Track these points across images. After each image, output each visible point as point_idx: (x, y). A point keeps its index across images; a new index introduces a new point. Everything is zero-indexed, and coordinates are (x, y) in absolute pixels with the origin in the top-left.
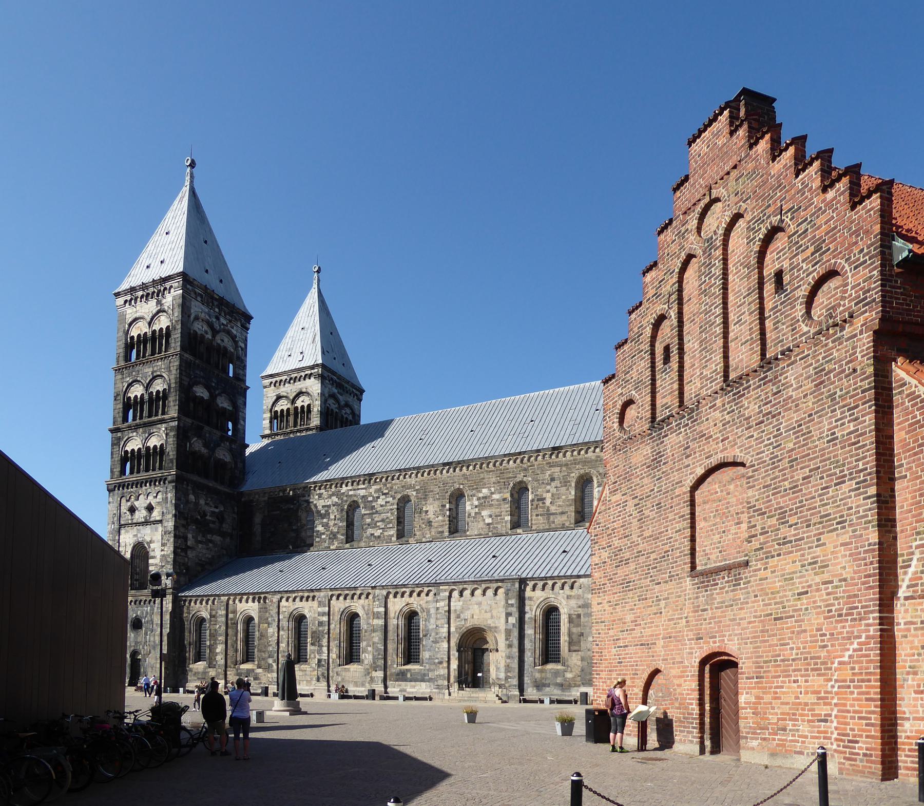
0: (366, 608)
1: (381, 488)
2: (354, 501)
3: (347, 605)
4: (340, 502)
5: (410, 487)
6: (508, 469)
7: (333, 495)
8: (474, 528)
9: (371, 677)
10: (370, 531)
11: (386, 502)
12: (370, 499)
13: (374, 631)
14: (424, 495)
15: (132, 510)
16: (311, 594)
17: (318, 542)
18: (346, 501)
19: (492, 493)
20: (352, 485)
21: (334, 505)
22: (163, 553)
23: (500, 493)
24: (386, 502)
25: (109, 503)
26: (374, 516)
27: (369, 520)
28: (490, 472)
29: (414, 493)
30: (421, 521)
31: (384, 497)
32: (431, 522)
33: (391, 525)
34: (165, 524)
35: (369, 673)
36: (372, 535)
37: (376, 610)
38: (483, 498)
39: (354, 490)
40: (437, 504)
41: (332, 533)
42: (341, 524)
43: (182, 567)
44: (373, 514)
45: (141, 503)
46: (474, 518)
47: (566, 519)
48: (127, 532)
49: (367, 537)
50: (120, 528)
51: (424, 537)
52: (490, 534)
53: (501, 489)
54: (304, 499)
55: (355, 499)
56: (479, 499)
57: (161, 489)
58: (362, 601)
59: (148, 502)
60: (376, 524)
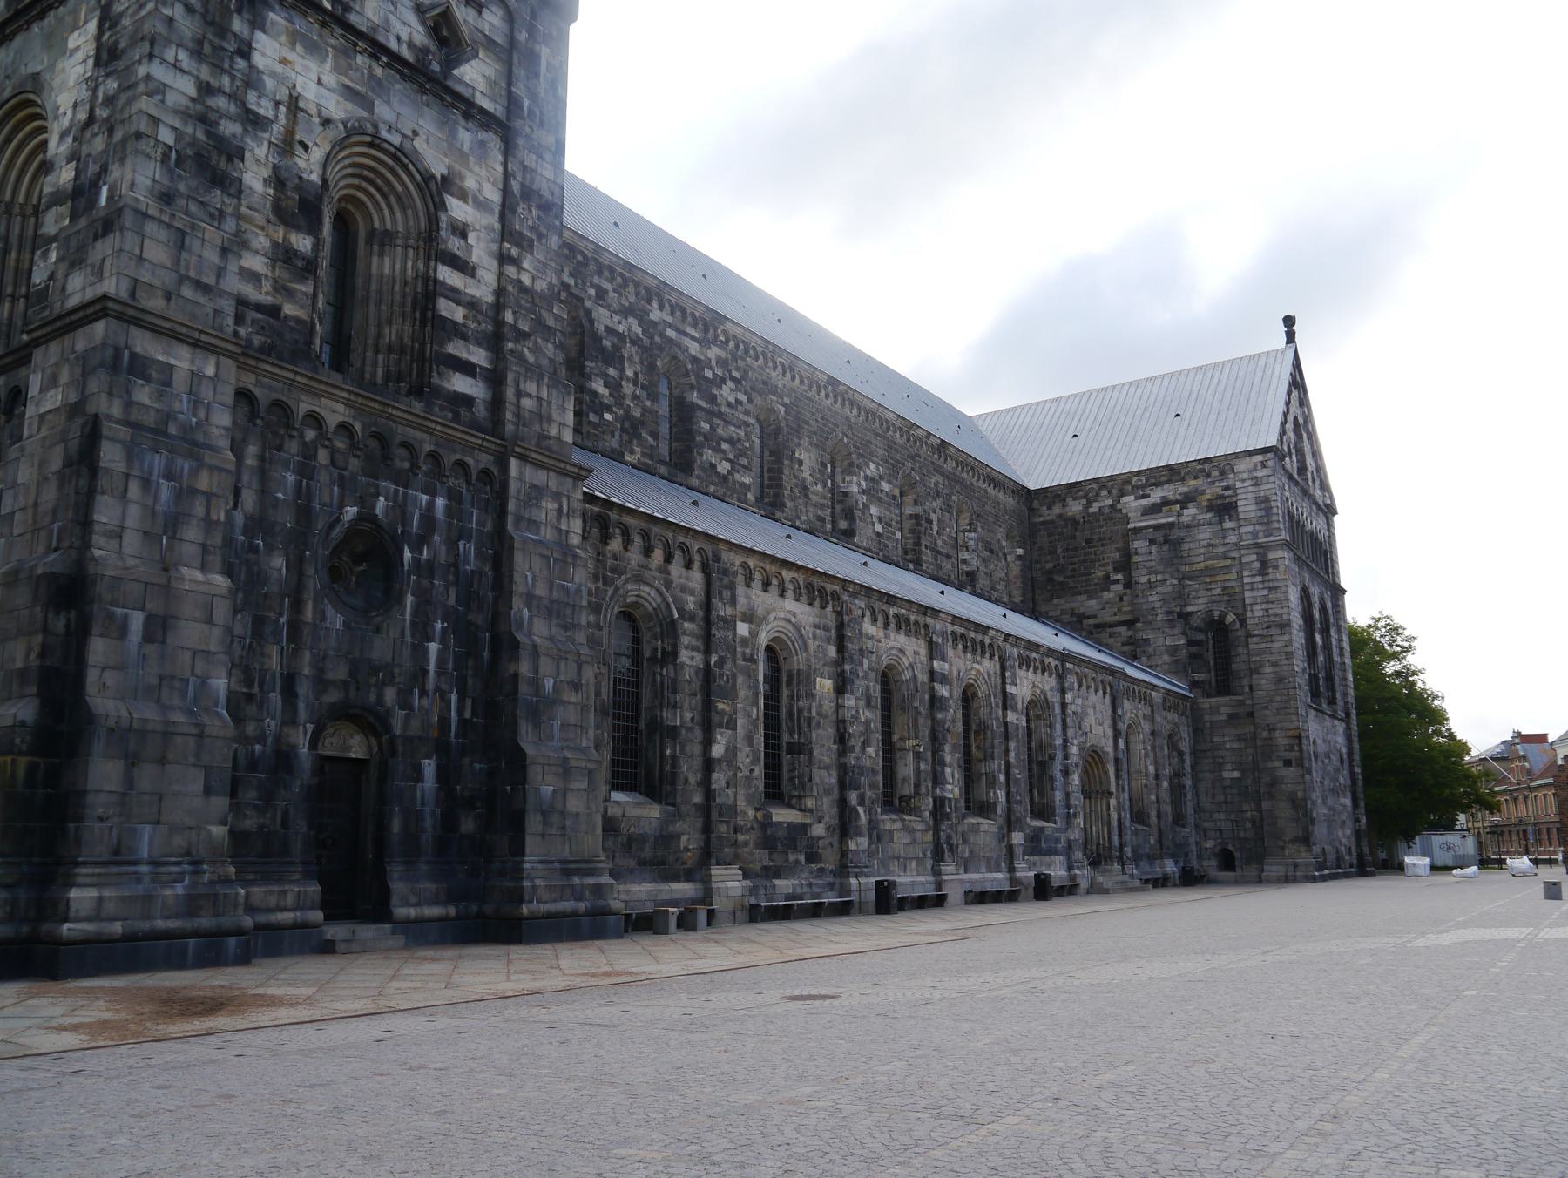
1: (727, 360)
10: (708, 455)
12: (708, 374)
16: (921, 619)
18: (661, 349)
19: (881, 478)
21: (633, 343)
24: (737, 400)
29: (782, 409)
30: (794, 480)
39: (678, 330)
41: (628, 415)
42: (648, 403)
49: (702, 468)
56: (866, 478)
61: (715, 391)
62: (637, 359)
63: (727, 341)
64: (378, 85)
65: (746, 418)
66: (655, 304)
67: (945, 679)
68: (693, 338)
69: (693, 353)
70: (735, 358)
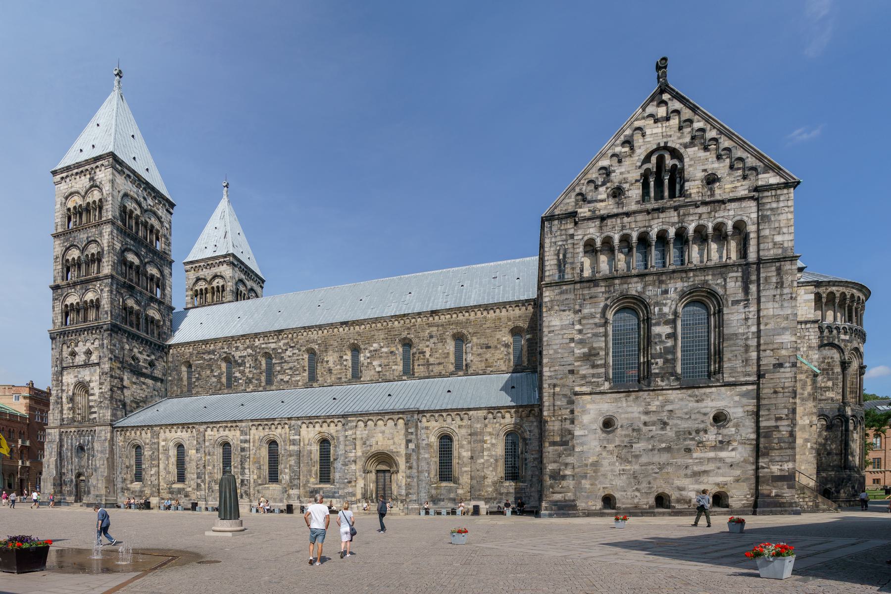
0: (283, 436)
1: (288, 342)
2: (266, 353)
3: (266, 434)
4: (254, 353)
5: (314, 341)
6: (394, 328)
7: (248, 347)
8: (367, 375)
9: (288, 495)
10: (280, 377)
11: (293, 354)
12: (280, 351)
13: (291, 456)
14: (326, 346)
15: (73, 354)
16: (234, 425)
17: (236, 386)
18: (259, 353)
19: (381, 347)
20: (264, 340)
21: (249, 356)
22: (101, 391)
23: (388, 347)
24: (293, 354)
25: (52, 349)
26: (283, 365)
27: (278, 368)
28: (380, 330)
29: (317, 347)
30: (323, 370)
31: (291, 349)
32: (332, 370)
33: (298, 372)
34: (103, 366)
35: (286, 491)
36: (282, 380)
37: (292, 438)
38: (374, 351)
39: (266, 343)
40: (336, 355)
43: (119, 403)
44: (282, 363)
45: (81, 349)
46: (367, 367)
47: (442, 368)
48: (69, 373)
50: (62, 370)
51: (326, 382)
52: (380, 380)
53: (388, 344)
54: (223, 350)
55: (267, 351)
56: (370, 352)
57: (98, 337)
58: (279, 430)
59: (86, 348)
60: (284, 371)
61: (282, 355)
62: (250, 360)
63: (287, 337)
64: (79, 372)
65: (298, 358)
66: (257, 340)
67: (246, 441)
68: (273, 343)
69: (272, 347)
70: (292, 339)
